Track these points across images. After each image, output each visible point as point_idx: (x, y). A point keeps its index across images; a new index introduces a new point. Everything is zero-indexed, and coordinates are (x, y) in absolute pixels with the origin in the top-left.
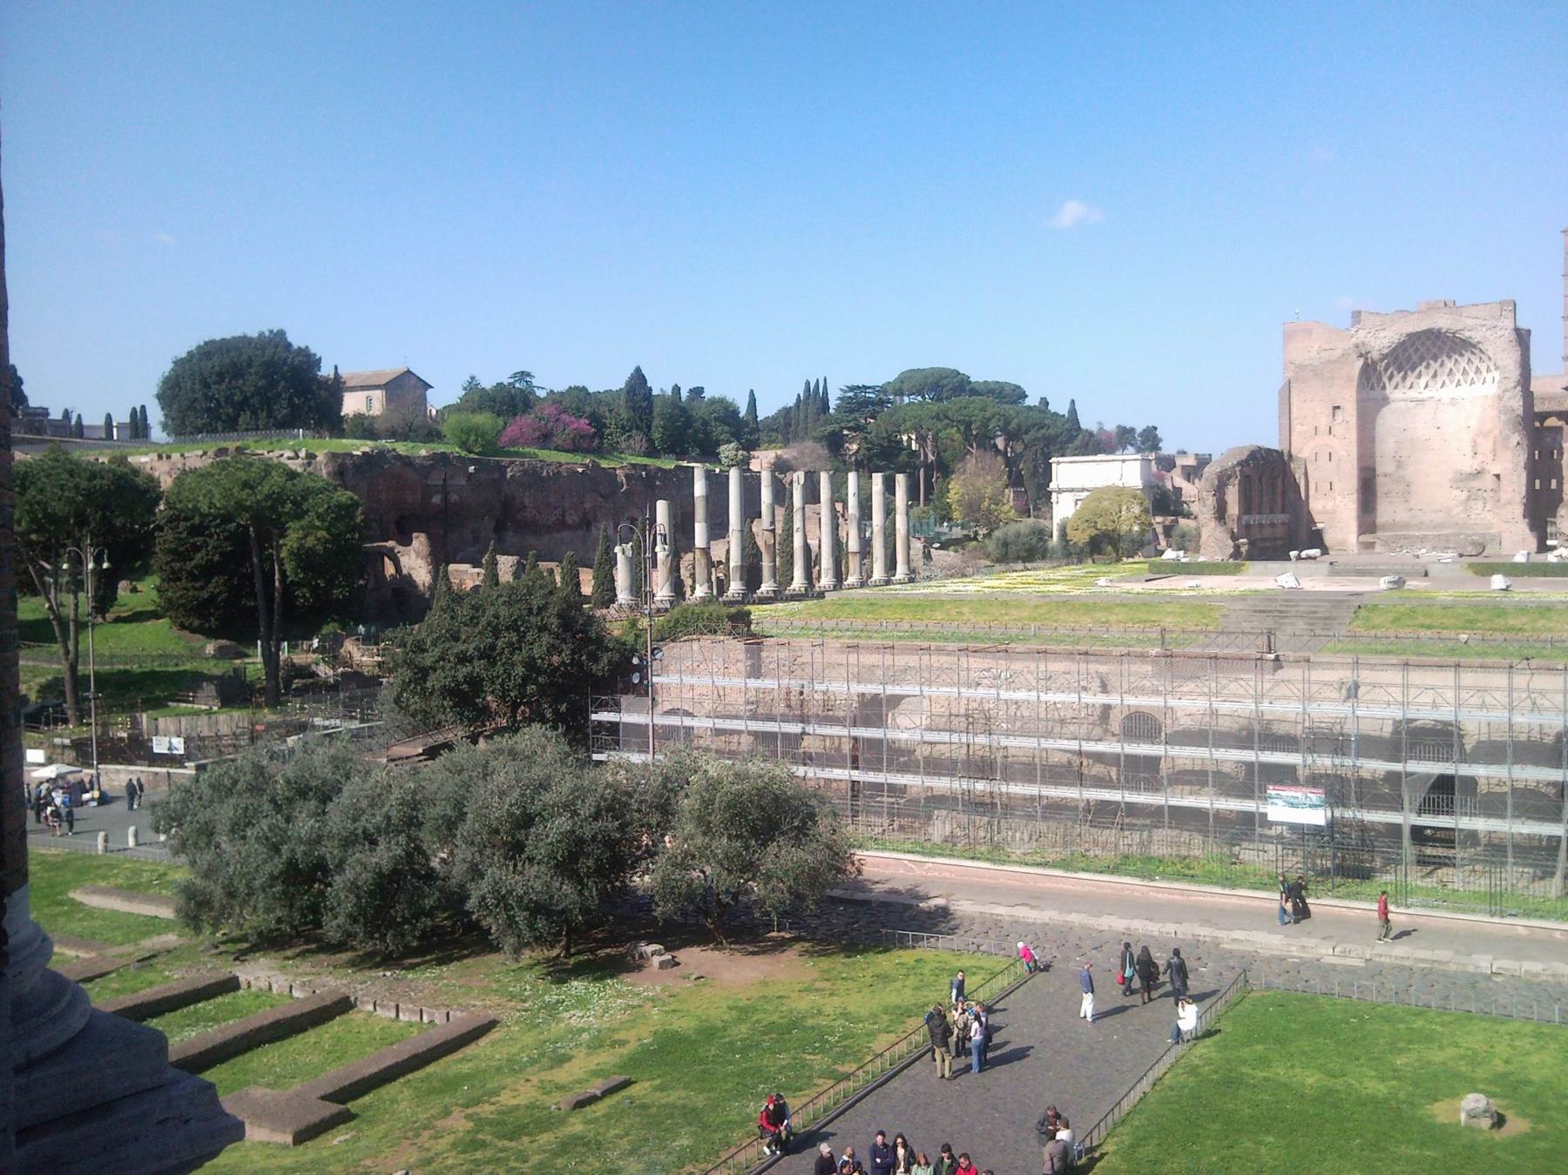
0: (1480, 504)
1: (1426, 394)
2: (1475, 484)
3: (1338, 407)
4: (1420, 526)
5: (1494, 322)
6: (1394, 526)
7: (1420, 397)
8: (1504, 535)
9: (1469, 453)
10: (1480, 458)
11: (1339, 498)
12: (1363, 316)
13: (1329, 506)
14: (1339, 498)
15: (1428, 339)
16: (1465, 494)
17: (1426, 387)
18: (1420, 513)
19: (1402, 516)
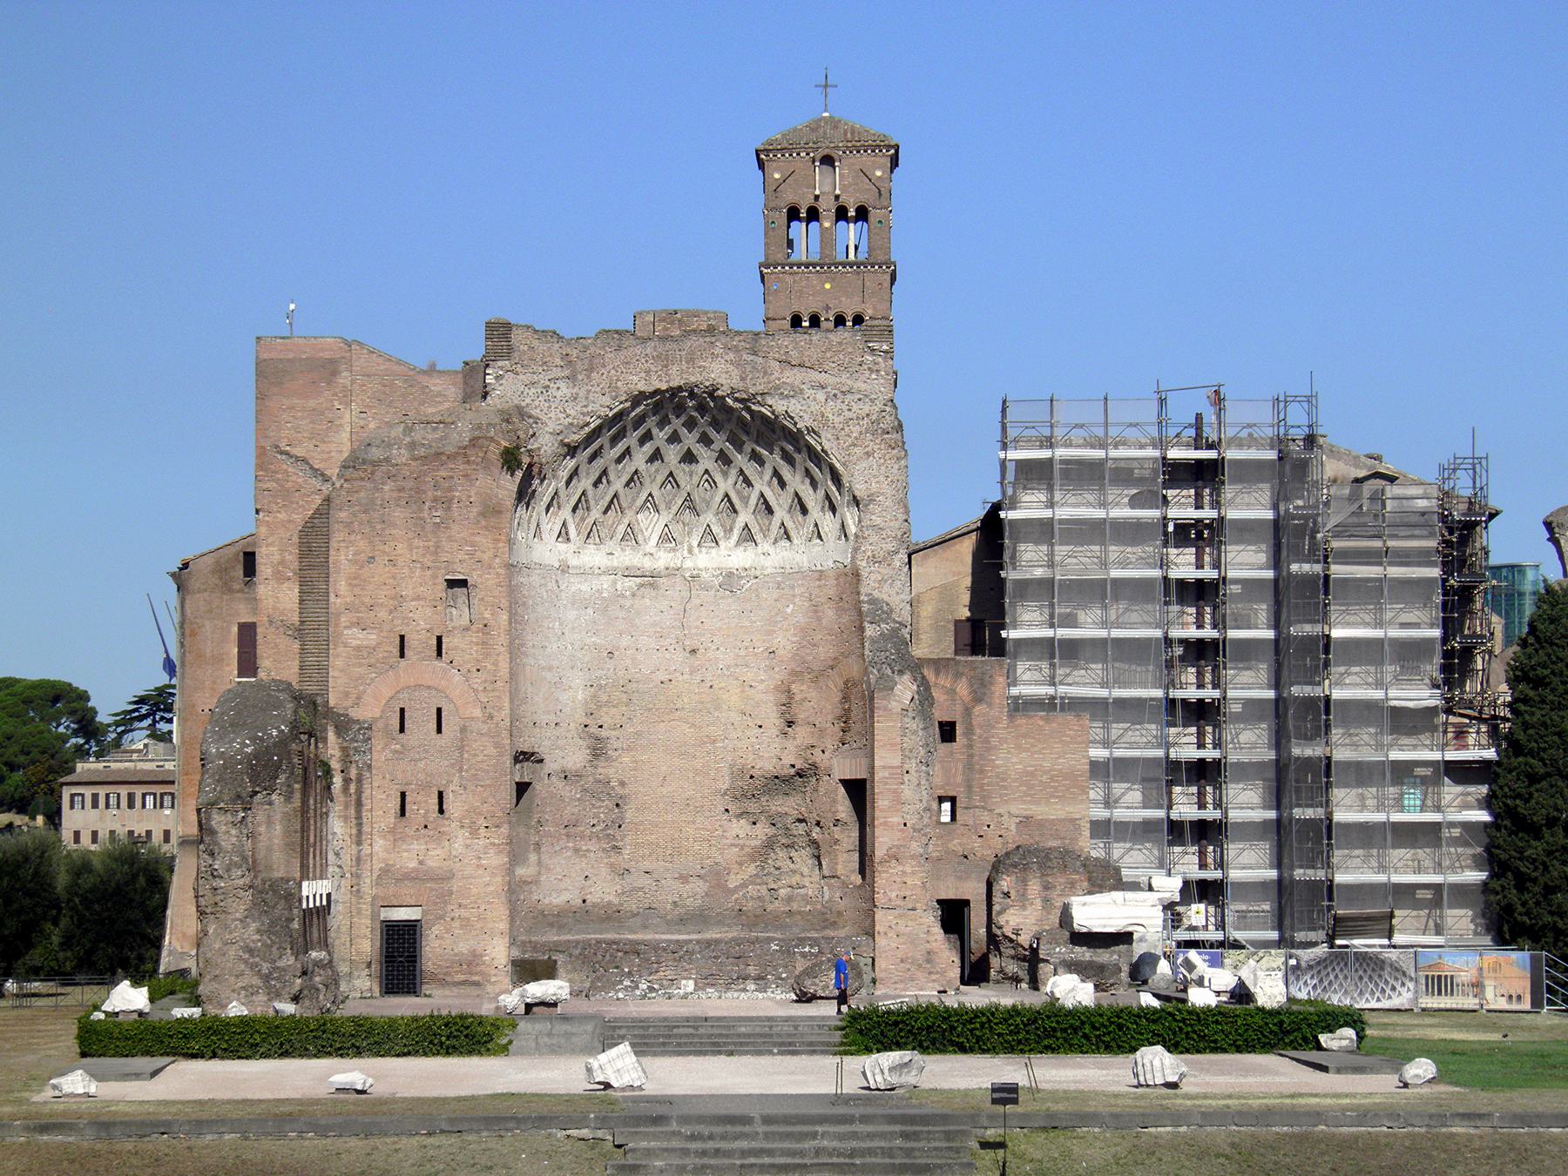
0: (803, 858)
1: (664, 559)
2: (788, 805)
3: (463, 583)
4: (648, 914)
5: (845, 380)
6: (584, 913)
7: (648, 564)
8: (881, 941)
9: (773, 721)
10: (802, 734)
11: (460, 842)
12: (517, 337)
13: (435, 858)
14: (460, 842)
15: (680, 409)
16: (763, 831)
17: (667, 538)
18: (646, 881)
19: (604, 891)
